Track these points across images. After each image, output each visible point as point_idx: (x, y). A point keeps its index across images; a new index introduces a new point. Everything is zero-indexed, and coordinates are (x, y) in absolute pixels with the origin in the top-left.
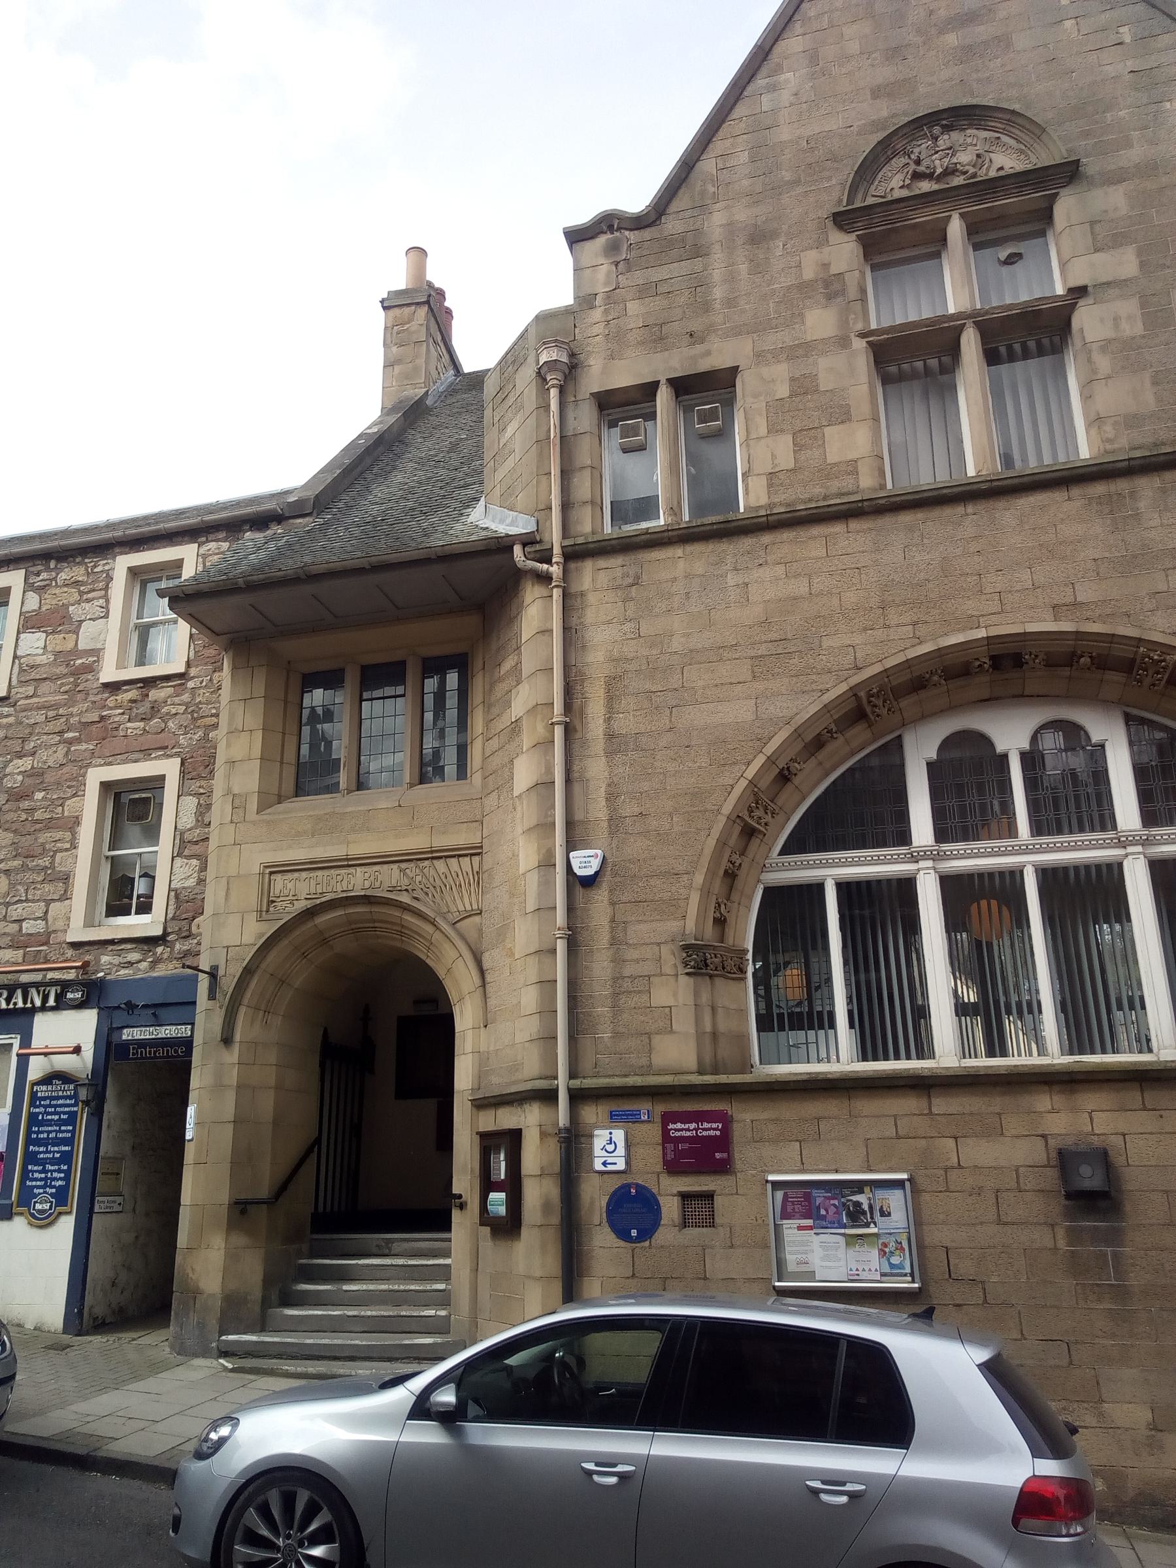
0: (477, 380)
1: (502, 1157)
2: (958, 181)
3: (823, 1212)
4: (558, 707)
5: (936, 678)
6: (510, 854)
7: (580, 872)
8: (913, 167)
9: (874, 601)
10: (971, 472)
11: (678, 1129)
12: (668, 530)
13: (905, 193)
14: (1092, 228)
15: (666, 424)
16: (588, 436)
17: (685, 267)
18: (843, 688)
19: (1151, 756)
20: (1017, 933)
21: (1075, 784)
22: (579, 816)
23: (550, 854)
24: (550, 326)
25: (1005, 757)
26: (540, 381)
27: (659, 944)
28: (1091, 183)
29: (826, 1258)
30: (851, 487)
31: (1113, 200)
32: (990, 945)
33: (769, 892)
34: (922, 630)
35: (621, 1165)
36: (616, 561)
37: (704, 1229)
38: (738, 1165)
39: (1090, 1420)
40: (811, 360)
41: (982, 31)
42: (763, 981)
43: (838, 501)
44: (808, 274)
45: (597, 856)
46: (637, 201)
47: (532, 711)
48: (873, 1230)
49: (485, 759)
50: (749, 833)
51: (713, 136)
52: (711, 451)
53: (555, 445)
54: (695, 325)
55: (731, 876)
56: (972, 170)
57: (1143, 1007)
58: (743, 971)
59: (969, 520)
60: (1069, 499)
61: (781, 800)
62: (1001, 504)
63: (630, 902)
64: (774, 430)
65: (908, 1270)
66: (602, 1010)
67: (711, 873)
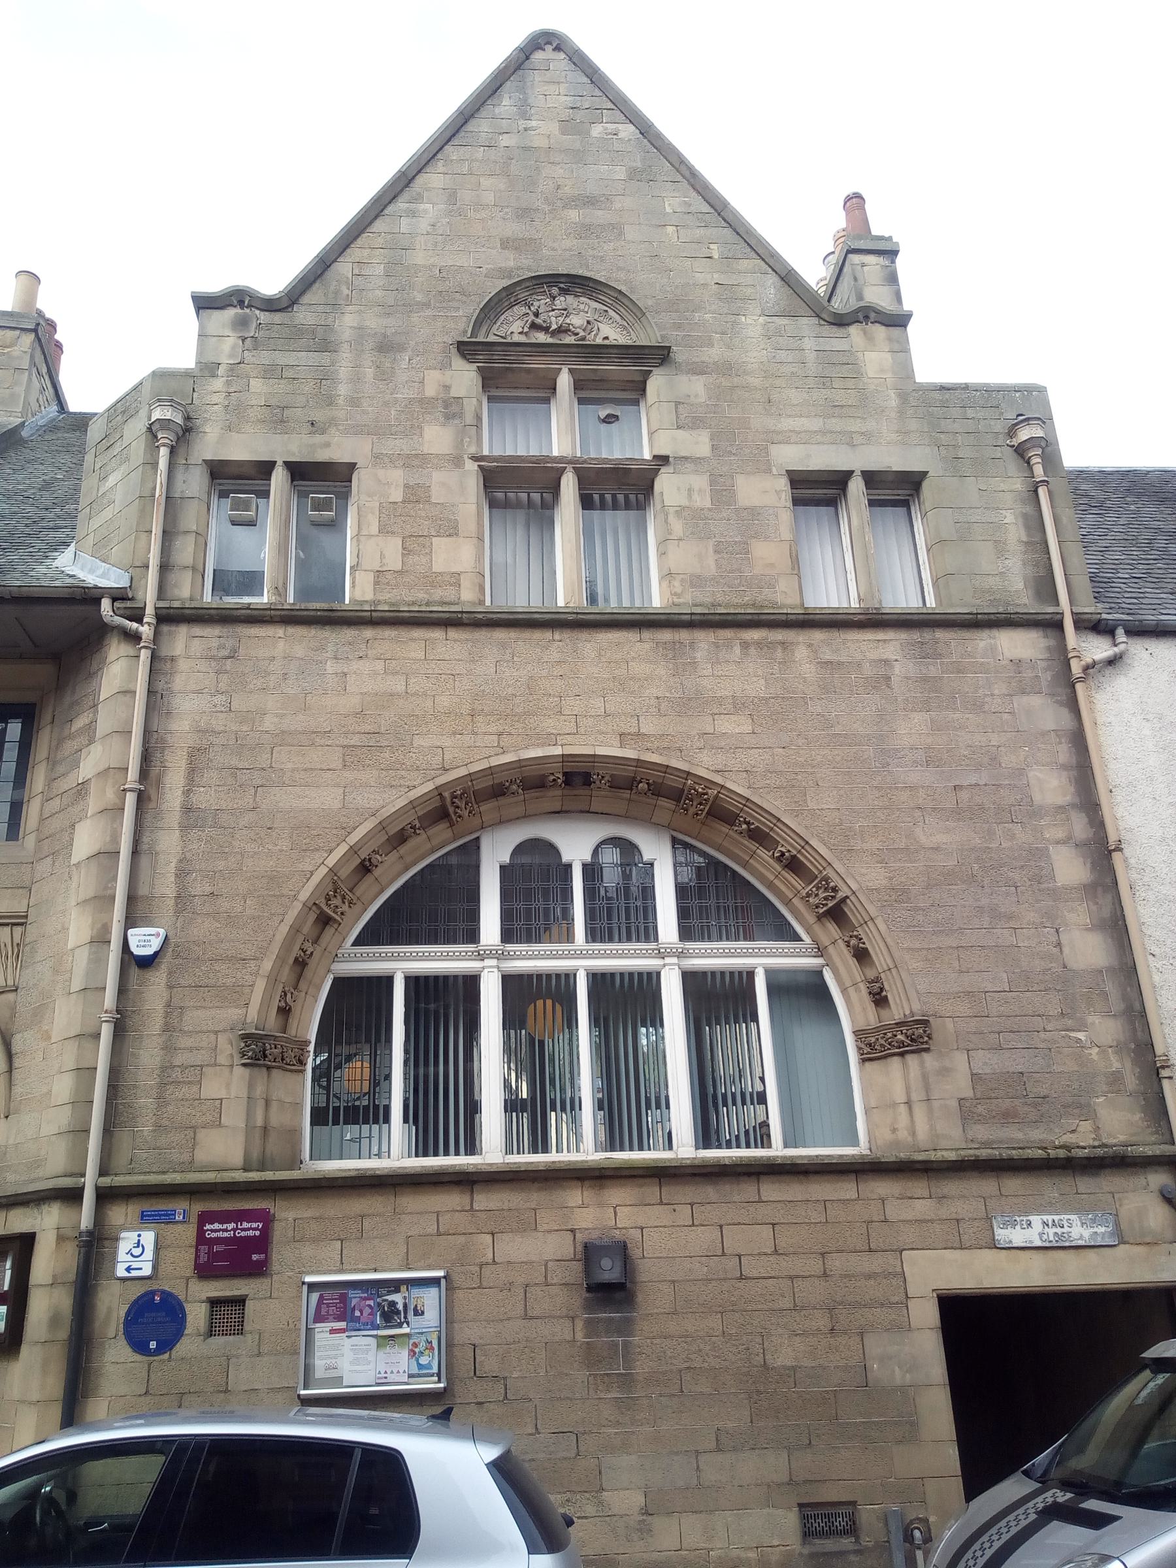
0: (82, 422)
1: (8, 1264)
2: (569, 340)
3: (357, 1313)
4: (133, 773)
5: (514, 787)
6: (59, 927)
7: (137, 951)
8: (532, 317)
9: (465, 709)
10: (561, 603)
11: (215, 1230)
12: (270, 609)
13: (523, 339)
14: (676, 408)
15: (278, 505)
16: (196, 501)
17: (313, 358)
18: (430, 786)
19: (687, 875)
20: (753, 1025)
21: (627, 897)
22: (143, 890)
23: (106, 929)
24: (164, 383)
25: (569, 867)
26: (150, 437)
27: (216, 1033)
28: (678, 368)
29: (356, 1362)
30: (452, 598)
31: (696, 388)
32: (542, 1043)
33: (337, 981)
34: (506, 741)
35: (147, 1270)
36: (212, 632)
37: (232, 1337)
38: (275, 1266)
39: (590, 1510)
40: (425, 471)
41: (600, 216)
42: (322, 1075)
43: (440, 609)
44: (430, 391)
45: (158, 935)
46: (272, 284)
47: (104, 774)
48: (405, 1330)
49: (42, 820)
50: (324, 921)
51: (352, 242)
52: (326, 538)
53: (159, 504)
54: (318, 415)
55: (301, 964)
56: (582, 334)
57: (668, 1107)
58: (302, 1062)
59: (557, 644)
60: (641, 641)
61: (359, 891)
62: (584, 635)
63: (190, 986)
64: (384, 530)
65: (435, 1370)
66: (145, 1102)
67: (280, 959)
